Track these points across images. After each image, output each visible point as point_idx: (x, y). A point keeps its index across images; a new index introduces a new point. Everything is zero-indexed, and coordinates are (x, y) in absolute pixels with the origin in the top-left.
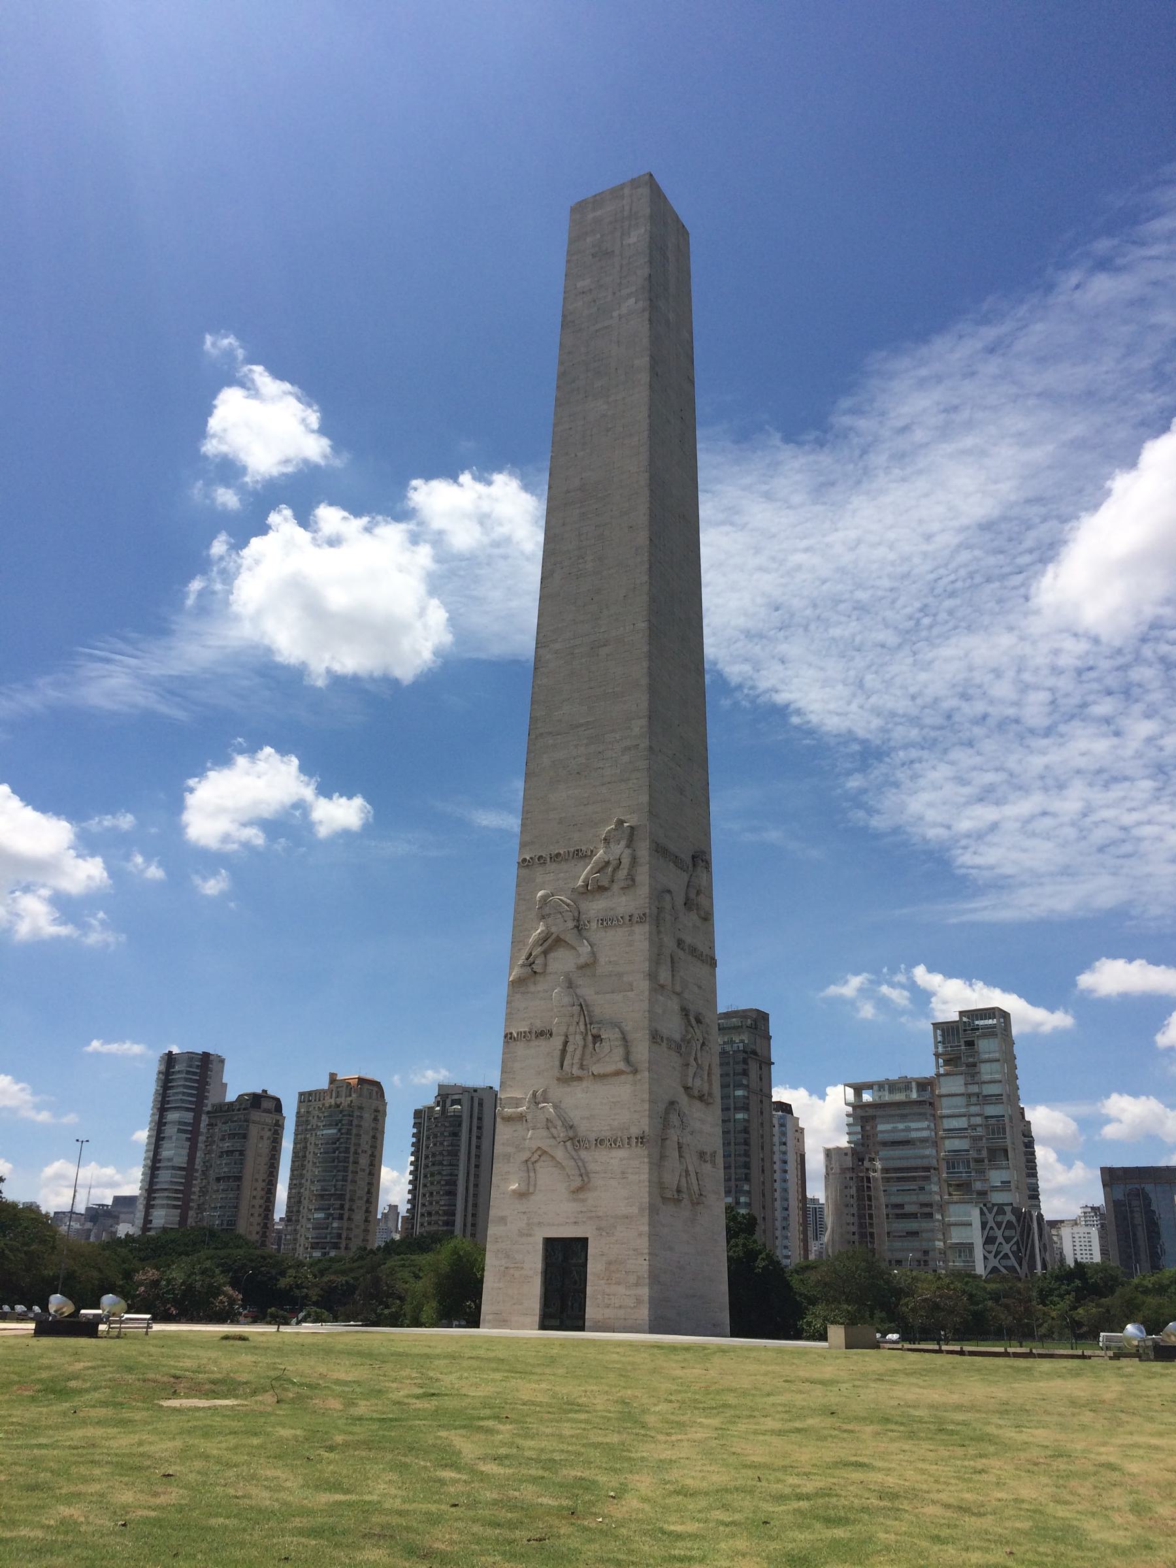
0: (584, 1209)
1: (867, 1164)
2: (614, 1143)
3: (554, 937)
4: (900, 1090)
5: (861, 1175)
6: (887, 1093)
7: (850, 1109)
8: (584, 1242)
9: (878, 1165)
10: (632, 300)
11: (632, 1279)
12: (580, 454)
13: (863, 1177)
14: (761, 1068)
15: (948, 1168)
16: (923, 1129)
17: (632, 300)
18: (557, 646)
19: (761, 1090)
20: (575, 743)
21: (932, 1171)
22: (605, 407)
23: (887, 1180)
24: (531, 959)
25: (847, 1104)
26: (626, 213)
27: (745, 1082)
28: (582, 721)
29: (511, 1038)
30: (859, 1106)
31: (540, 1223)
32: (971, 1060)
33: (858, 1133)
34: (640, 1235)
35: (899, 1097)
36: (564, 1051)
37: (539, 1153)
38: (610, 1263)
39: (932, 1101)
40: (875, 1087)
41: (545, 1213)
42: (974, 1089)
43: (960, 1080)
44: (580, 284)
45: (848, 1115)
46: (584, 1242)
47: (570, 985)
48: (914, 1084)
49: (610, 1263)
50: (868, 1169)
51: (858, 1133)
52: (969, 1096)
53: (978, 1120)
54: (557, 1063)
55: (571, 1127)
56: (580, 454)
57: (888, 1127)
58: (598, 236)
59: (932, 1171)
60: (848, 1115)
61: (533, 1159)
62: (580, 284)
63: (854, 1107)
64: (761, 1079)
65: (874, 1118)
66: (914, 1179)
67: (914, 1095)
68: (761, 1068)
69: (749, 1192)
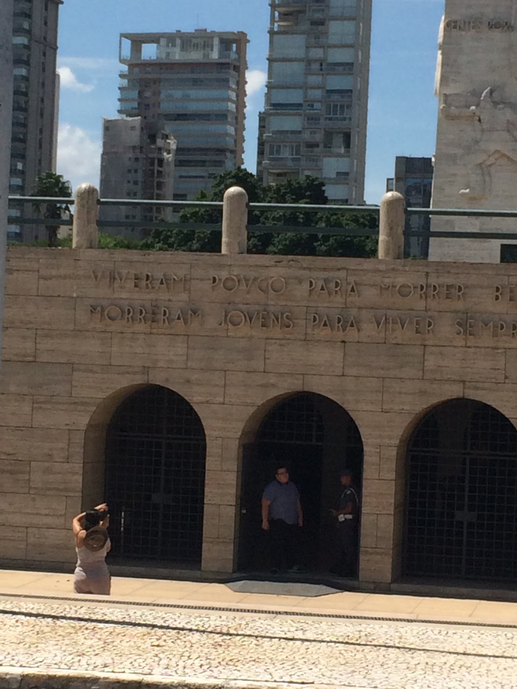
1: (160, 142)
4: (196, 46)
5: (151, 156)
6: (177, 49)
7: (125, 68)
9: (173, 144)
13: (153, 159)
14: (46, 9)
15: (271, 153)
16: (198, 100)
19: (45, 38)
21: (228, 154)
23: (180, 163)
25: (122, 61)
27: (26, 26)
29: (455, 27)
30: (137, 65)
32: (318, 16)
33: (133, 100)
35: (195, 56)
39: (237, 64)
40: (163, 41)
42: (317, 53)
43: (299, 40)
45: (122, 76)
48: (216, 41)
50: (160, 149)
51: (133, 100)
52: (309, 62)
53: (318, 94)
57: (178, 94)
59: (228, 154)
60: (122, 76)
61: (488, 163)
63: (131, 66)
64: (46, 24)
65: (156, 81)
66: (203, 163)
67: (215, 55)
68: (46, 9)
69: (23, 172)
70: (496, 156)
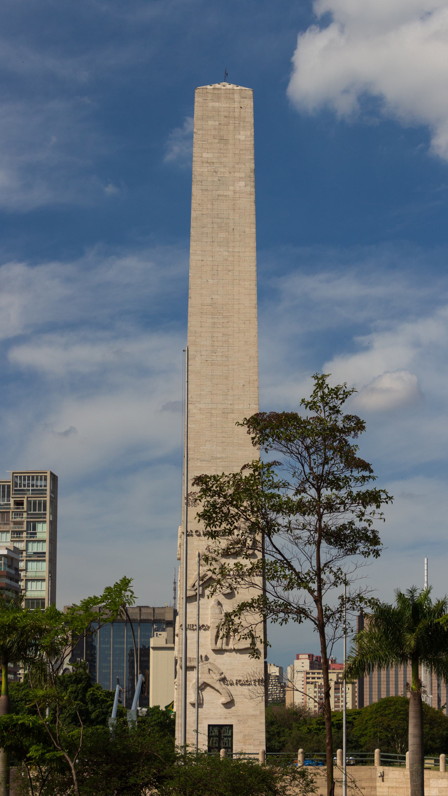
0: (230, 712)
2: (247, 683)
3: (207, 577)
8: (231, 726)
10: (242, 184)
11: (257, 742)
12: (211, 281)
17: (242, 184)
18: (202, 406)
20: (215, 468)
22: (226, 254)
24: (195, 588)
26: (237, 114)
28: (219, 456)
31: (206, 718)
34: (261, 723)
36: (217, 637)
37: (205, 685)
38: (245, 736)
41: (208, 713)
44: (205, 155)
46: (231, 726)
47: (219, 604)
49: (245, 736)
54: (214, 642)
55: (222, 673)
56: (211, 281)
58: (217, 123)
62: (205, 155)
70: (205, 685)
